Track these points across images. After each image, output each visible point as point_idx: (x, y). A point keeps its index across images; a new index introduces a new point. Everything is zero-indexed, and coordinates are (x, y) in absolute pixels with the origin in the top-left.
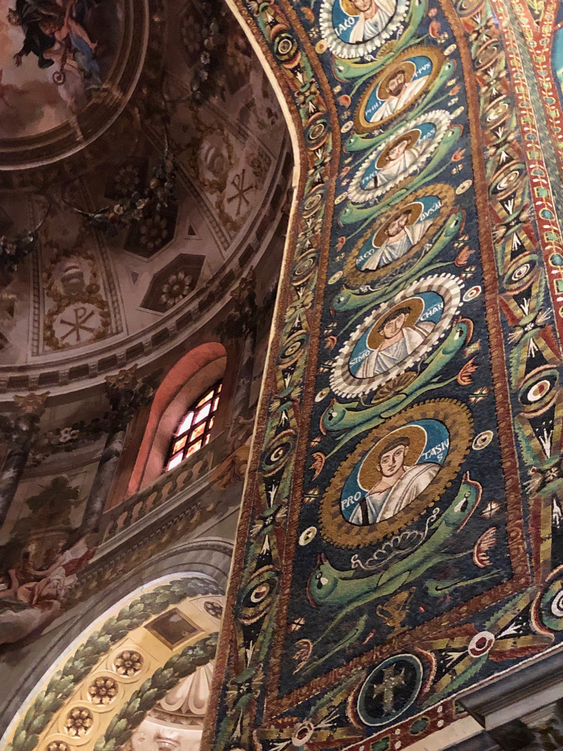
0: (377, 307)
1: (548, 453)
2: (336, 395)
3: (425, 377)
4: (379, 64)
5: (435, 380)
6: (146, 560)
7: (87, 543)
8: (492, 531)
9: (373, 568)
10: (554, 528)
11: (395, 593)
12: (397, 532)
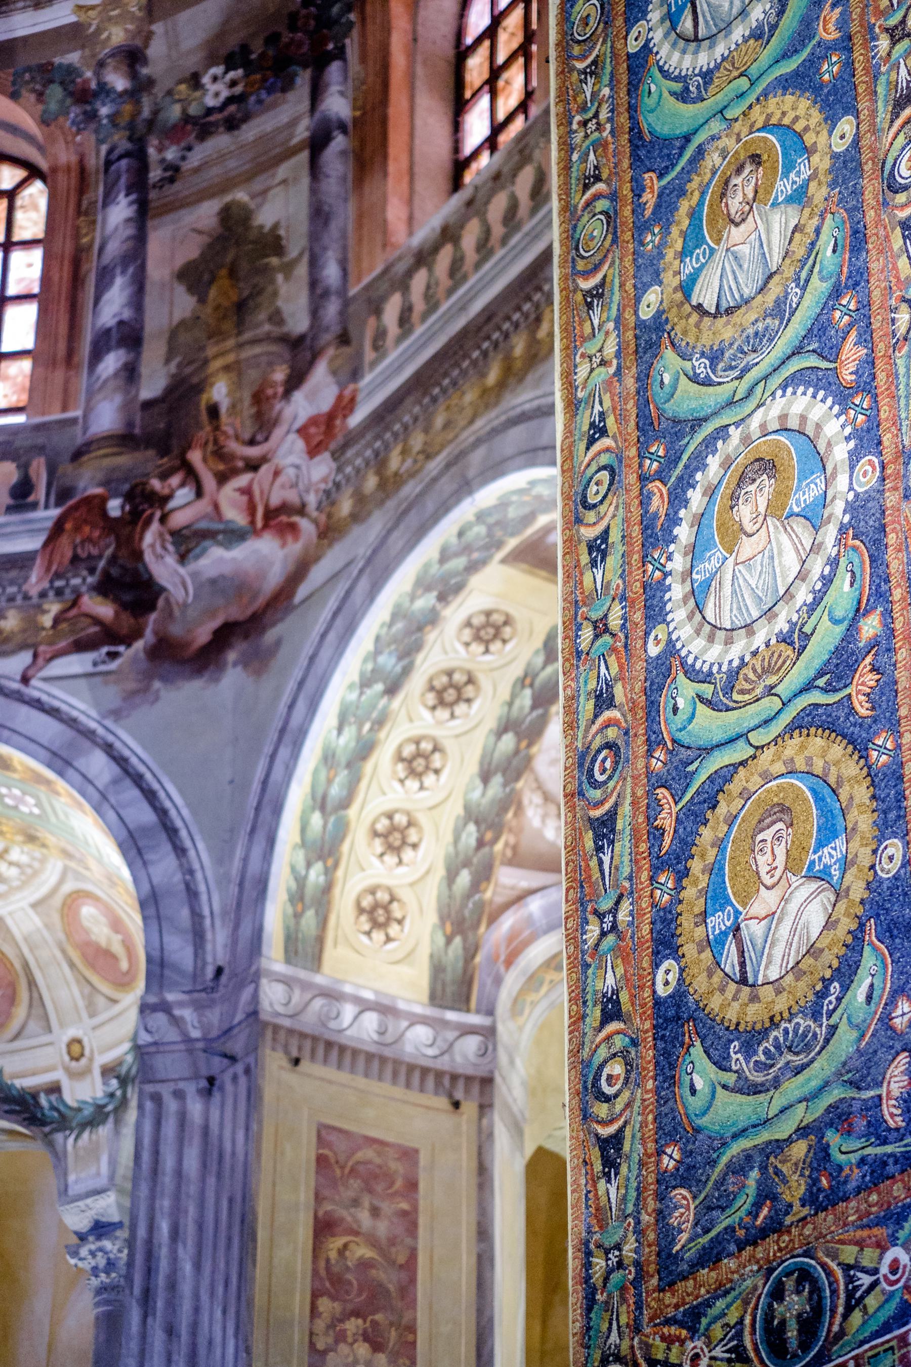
3: (806, 668)
5: (821, 682)
6: (464, 428)
7: (334, 373)
11: (789, 1141)
12: (786, 1015)
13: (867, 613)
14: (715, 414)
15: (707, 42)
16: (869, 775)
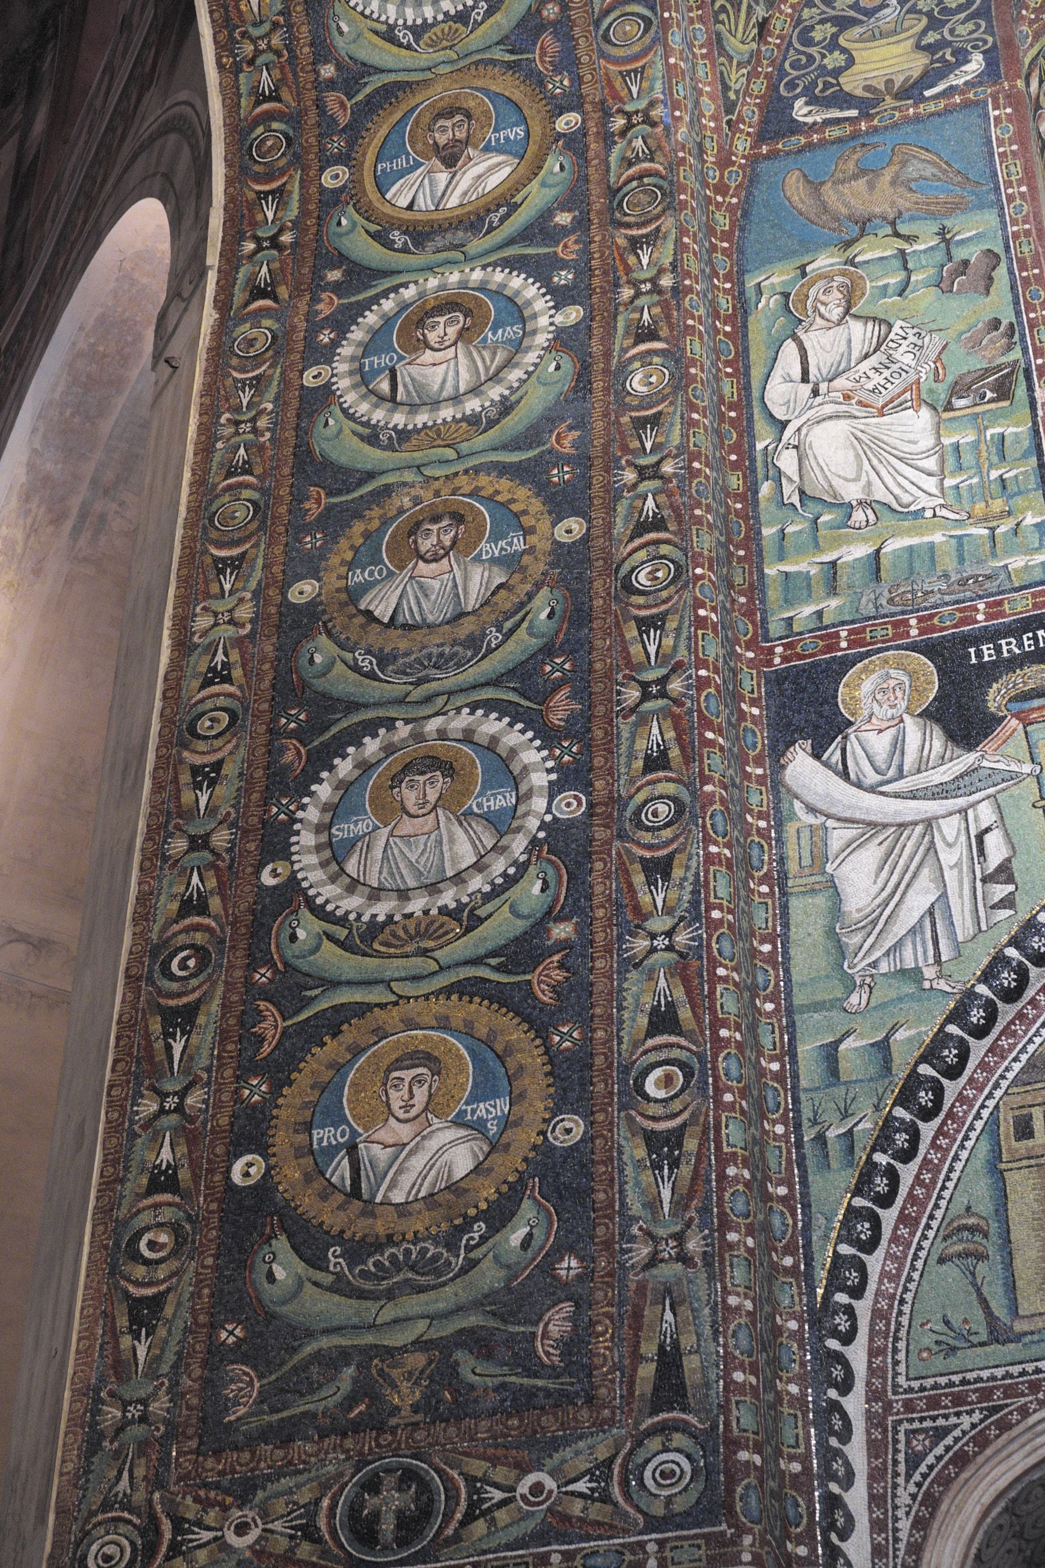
0: (390, 724)
1: (666, 1210)
2: (304, 891)
3: (476, 946)
4: (423, 64)
5: (493, 961)
8: (568, 1307)
9: (368, 1286)
10: (661, 1347)
11: (404, 1349)
12: (410, 1236)
13: (560, 919)
14: (377, 705)
15: (407, 408)
16: (546, 1053)
